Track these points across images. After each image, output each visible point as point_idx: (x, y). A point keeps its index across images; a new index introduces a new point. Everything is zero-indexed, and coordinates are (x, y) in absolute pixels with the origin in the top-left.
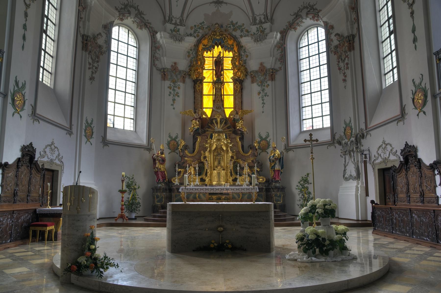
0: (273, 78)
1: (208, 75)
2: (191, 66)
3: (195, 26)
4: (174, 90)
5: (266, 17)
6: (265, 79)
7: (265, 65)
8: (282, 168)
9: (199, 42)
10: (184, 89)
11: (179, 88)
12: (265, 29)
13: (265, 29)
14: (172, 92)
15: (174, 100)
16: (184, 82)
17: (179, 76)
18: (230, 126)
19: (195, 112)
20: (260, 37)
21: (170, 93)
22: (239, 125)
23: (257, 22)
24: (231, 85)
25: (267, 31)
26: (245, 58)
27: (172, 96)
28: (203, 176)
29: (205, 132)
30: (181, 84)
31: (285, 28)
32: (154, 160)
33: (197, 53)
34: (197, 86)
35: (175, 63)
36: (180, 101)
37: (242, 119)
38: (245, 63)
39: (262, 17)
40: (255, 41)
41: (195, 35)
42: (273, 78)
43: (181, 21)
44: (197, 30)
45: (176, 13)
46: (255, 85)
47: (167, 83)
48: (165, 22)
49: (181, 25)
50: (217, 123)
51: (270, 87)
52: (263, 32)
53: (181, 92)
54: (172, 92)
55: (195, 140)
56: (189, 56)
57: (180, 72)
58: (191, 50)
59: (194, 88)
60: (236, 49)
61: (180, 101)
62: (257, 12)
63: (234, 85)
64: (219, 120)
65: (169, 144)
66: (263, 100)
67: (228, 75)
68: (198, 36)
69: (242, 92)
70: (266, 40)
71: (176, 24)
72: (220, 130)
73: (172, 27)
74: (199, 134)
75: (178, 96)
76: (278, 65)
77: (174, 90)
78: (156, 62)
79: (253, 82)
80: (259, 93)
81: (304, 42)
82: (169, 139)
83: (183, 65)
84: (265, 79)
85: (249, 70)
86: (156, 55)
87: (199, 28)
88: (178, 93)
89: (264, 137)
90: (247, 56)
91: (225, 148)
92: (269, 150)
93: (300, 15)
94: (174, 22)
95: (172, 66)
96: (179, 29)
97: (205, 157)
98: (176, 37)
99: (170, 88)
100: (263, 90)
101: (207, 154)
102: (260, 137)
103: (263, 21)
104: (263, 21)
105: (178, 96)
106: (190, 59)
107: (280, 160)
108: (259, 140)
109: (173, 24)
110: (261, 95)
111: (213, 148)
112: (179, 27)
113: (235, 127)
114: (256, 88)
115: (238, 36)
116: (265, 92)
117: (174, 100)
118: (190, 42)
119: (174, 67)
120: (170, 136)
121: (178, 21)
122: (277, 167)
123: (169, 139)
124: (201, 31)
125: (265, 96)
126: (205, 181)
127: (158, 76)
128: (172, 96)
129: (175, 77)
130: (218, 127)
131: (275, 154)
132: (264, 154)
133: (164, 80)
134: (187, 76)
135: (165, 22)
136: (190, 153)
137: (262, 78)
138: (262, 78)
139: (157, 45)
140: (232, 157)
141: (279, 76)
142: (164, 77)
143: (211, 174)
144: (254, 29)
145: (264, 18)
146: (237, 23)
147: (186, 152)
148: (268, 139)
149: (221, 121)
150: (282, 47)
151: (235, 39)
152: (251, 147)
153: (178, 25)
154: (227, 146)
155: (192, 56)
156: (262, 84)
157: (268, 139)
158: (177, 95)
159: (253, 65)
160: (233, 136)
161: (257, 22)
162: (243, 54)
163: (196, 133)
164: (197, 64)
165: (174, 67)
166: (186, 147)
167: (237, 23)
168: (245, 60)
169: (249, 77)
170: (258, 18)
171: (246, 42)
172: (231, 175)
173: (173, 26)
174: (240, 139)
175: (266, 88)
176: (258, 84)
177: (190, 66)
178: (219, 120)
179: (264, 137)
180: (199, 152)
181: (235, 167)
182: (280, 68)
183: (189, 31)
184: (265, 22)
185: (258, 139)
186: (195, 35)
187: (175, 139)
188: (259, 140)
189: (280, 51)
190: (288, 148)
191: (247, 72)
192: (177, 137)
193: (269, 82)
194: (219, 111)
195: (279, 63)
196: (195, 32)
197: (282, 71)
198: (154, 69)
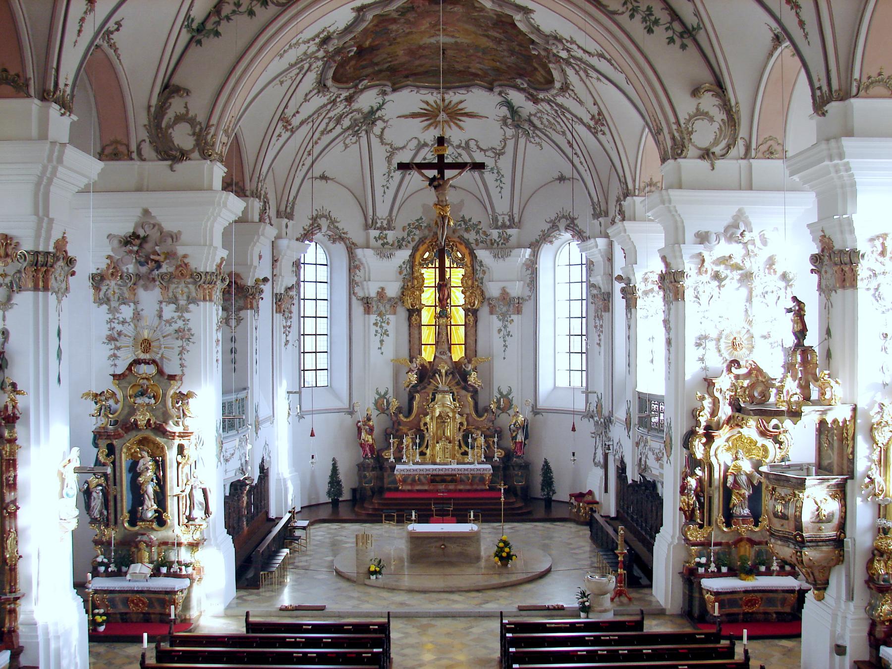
0: (519, 312)
1: (429, 296)
2: (404, 289)
3: (409, 225)
4: (381, 327)
5: (512, 219)
6: (508, 311)
7: (508, 290)
8: (526, 438)
9: (415, 249)
10: (396, 322)
11: (388, 323)
12: (510, 236)
13: (510, 236)
14: (380, 331)
15: (382, 341)
16: (395, 313)
17: (388, 306)
18: (459, 373)
19: (411, 361)
20: (501, 248)
21: (377, 331)
22: (473, 378)
23: (500, 224)
24: (462, 313)
25: (513, 240)
26: (481, 275)
27: (379, 335)
28: (423, 448)
29: (425, 388)
30: (392, 318)
31: (538, 238)
32: (359, 429)
33: (412, 267)
34: (413, 319)
35: (383, 289)
36: (389, 341)
37: (475, 369)
38: (482, 283)
39: (507, 218)
40: (495, 257)
41: (410, 239)
42: (519, 312)
43: (389, 222)
44: (411, 232)
45: (382, 212)
46: (495, 317)
47: (373, 318)
48: (367, 227)
49: (389, 228)
50: (440, 375)
51: (515, 323)
52: (507, 239)
53: (391, 328)
54: (380, 331)
55: (411, 399)
56: (400, 273)
57: (390, 300)
58: (404, 263)
59: (409, 319)
60: (467, 259)
61: (389, 341)
62: (499, 210)
63: (466, 316)
64: (443, 371)
65: (376, 403)
66: (505, 341)
67: (458, 297)
68: (413, 240)
69: (476, 326)
70: (509, 258)
71: (382, 228)
72: (447, 389)
73: (376, 233)
74: (418, 392)
75: (388, 335)
76: (527, 292)
77: (381, 327)
78: (357, 289)
79: (491, 313)
80: (500, 331)
81: (563, 258)
82: (377, 397)
83: (393, 290)
84: (508, 311)
85: (487, 295)
86: (357, 278)
87: (415, 228)
88: (386, 331)
89: (505, 393)
90: (484, 272)
91: (451, 415)
92: (511, 412)
93: (557, 226)
94: (378, 225)
95: (378, 292)
96: (386, 235)
97: (425, 424)
98: (385, 249)
99: (376, 324)
100: (505, 327)
101: (428, 419)
102: (501, 393)
103: (508, 223)
104: (508, 223)
105: (388, 335)
106: (402, 276)
107: (525, 427)
108: (499, 396)
109: (378, 229)
110: (502, 333)
111: (437, 414)
112: (385, 232)
113: (465, 380)
114: (496, 322)
115: (471, 241)
116: (508, 330)
117: (382, 341)
118: (404, 255)
119: (381, 294)
120: (378, 393)
121: (385, 222)
122: (520, 438)
123: (377, 397)
124: (417, 232)
125: (508, 335)
126: (425, 454)
127: (358, 308)
128: (379, 335)
129: (382, 308)
130: (442, 383)
131: (516, 421)
132: (504, 416)
133: (368, 313)
134: (399, 303)
135: (367, 227)
136: (406, 417)
137: (504, 309)
138: (504, 309)
139: (357, 263)
140: (461, 424)
141: (527, 308)
142: (368, 310)
143: (434, 447)
144: (495, 234)
145: (509, 220)
146: (470, 220)
147: (401, 415)
148: (510, 397)
149: (446, 373)
150: (532, 268)
151: (467, 244)
152: (487, 409)
153: (385, 229)
154: (453, 411)
155: (405, 272)
156: (503, 317)
157: (510, 397)
158: (386, 333)
159: (493, 290)
160: (463, 392)
161: (500, 224)
162: (478, 268)
163: (413, 392)
164: (412, 284)
165: (381, 294)
166: (399, 410)
167: (470, 220)
168: (482, 279)
169: (486, 303)
170: (500, 219)
171: (483, 254)
172: (460, 446)
173: (378, 232)
174: (472, 397)
175: (509, 325)
176: (498, 317)
177: (403, 287)
178: (443, 371)
179: (505, 393)
180: (417, 415)
181: (465, 437)
182: (530, 297)
183: (400, 234)
184: (510, 227)
185: (496, 394)
186: (410, 239)
187: (384, 397)
188: (499, 396)
189: (529, 272)
190: (536, 411)
191: (484, 299)
192: (386, 393)
193: (514, 317)
194: (444, 357)
195: (528, 289)
196: (408, 235)
197: (532, 302)
198: (354, 298)
